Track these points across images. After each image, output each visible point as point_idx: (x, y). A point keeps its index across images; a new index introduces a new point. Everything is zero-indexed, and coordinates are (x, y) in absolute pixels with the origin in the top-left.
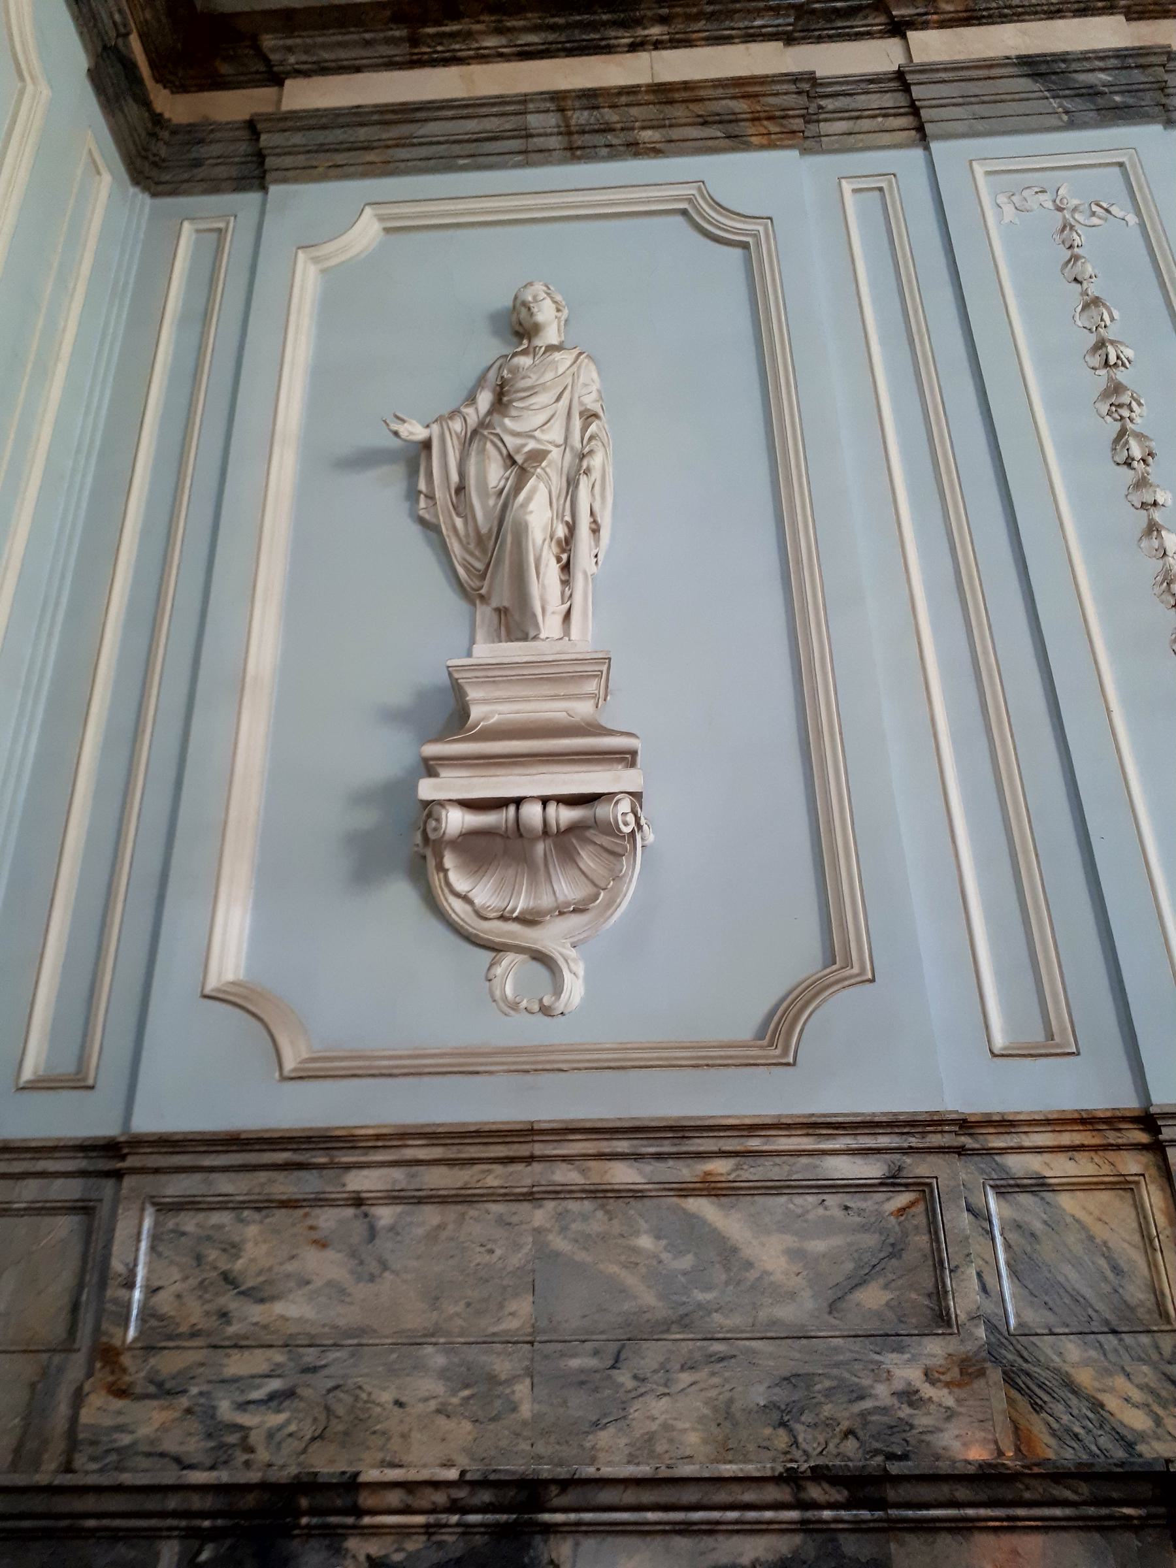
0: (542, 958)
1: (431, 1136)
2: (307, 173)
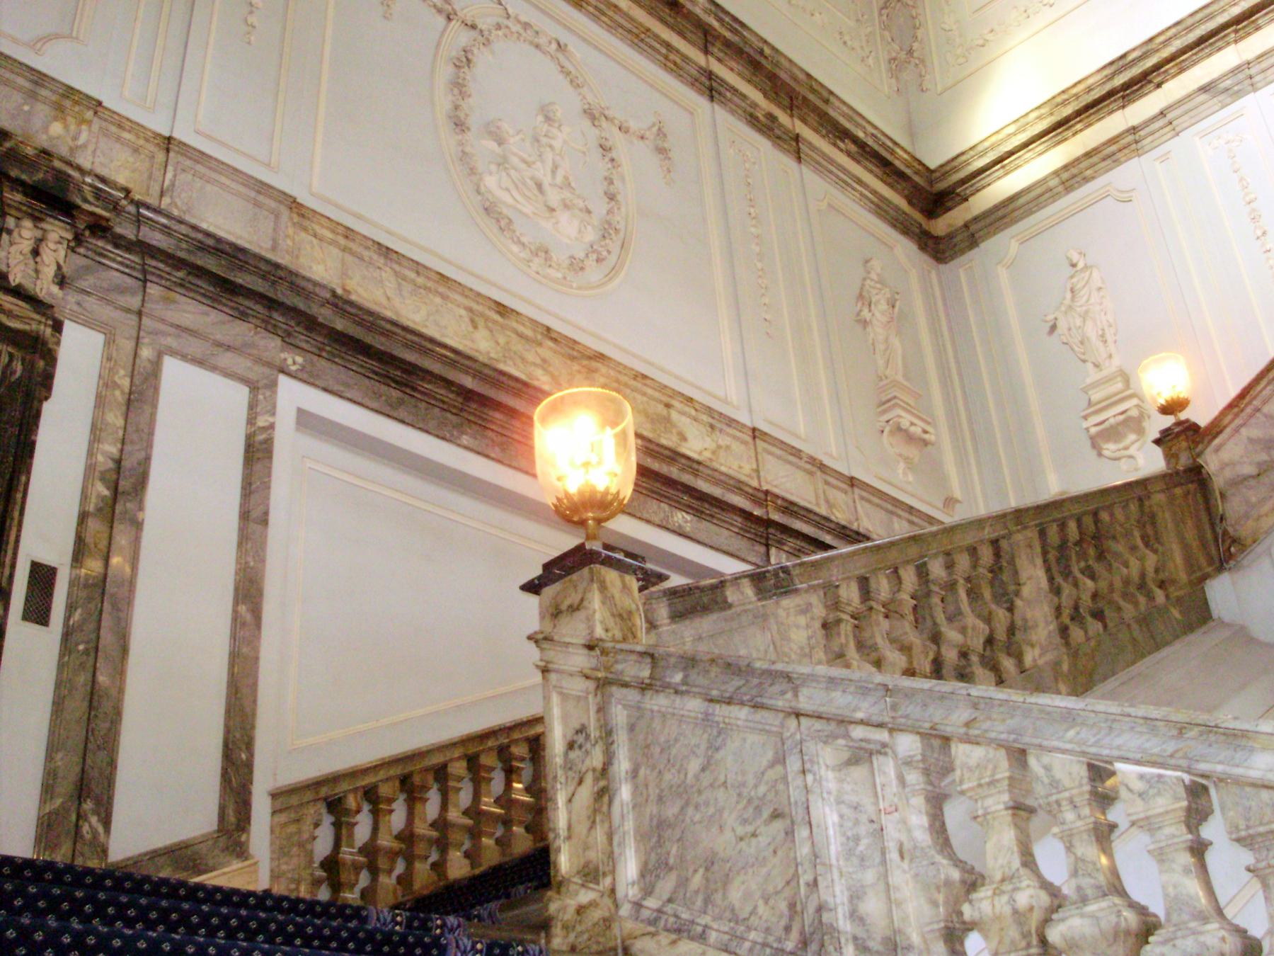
0: (1131, 457)
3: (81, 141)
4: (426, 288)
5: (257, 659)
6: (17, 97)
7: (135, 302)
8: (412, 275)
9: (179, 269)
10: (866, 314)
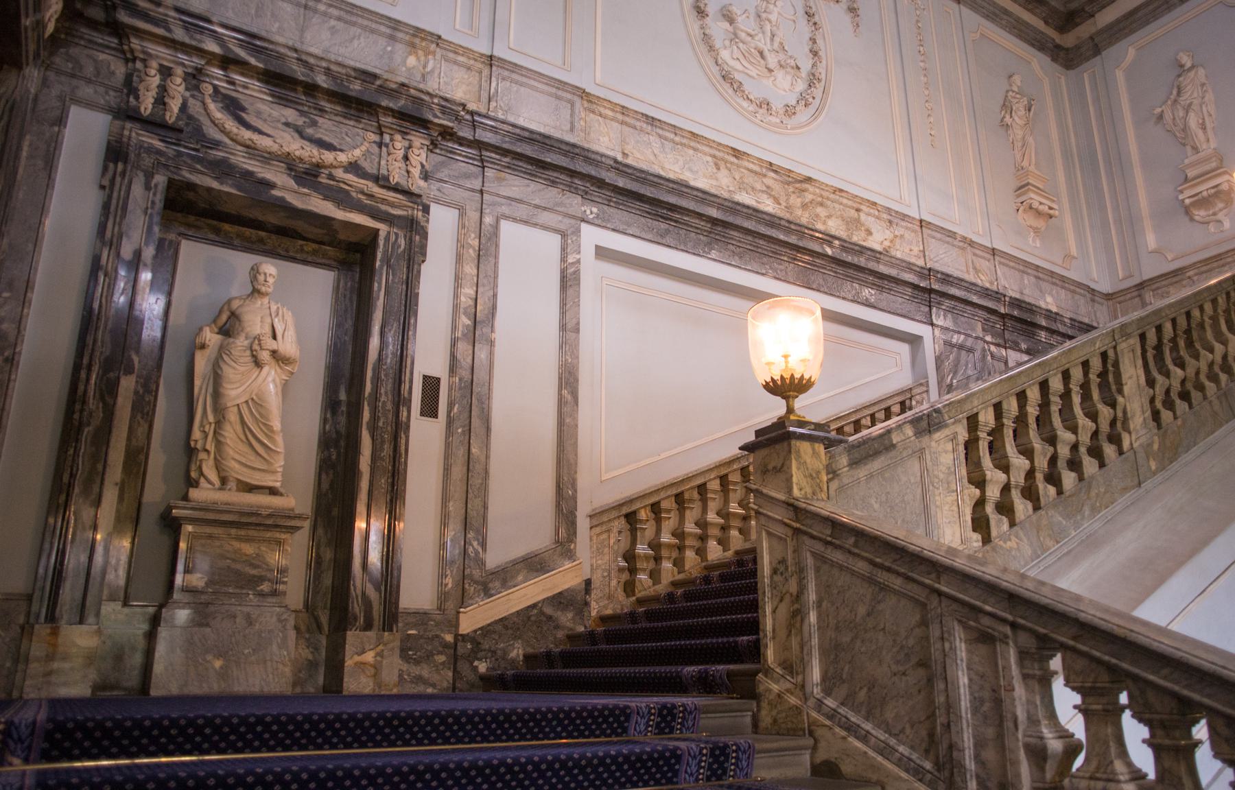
1: (1200, 262)
2: (1111, 44)
3: (429, 68)
4: (682, 144)
6: (382, 41)
7: (477, 184)
8: (672, 136)
9: (506, 156)
10: (1008, 120)
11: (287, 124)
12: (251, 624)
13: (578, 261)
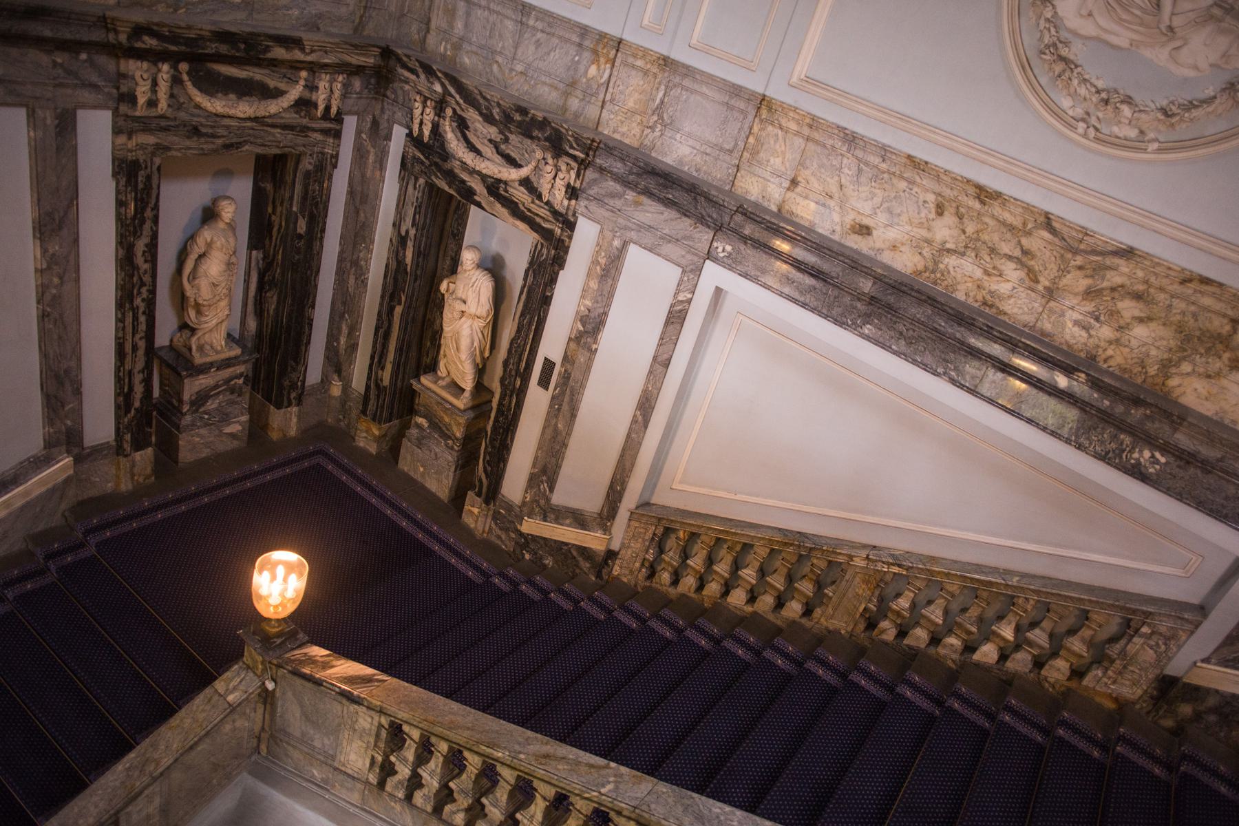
5: (640, 444)
6: (573, 50)
11: (490, 141)
12: (436, 459)
13: (689, 301)
